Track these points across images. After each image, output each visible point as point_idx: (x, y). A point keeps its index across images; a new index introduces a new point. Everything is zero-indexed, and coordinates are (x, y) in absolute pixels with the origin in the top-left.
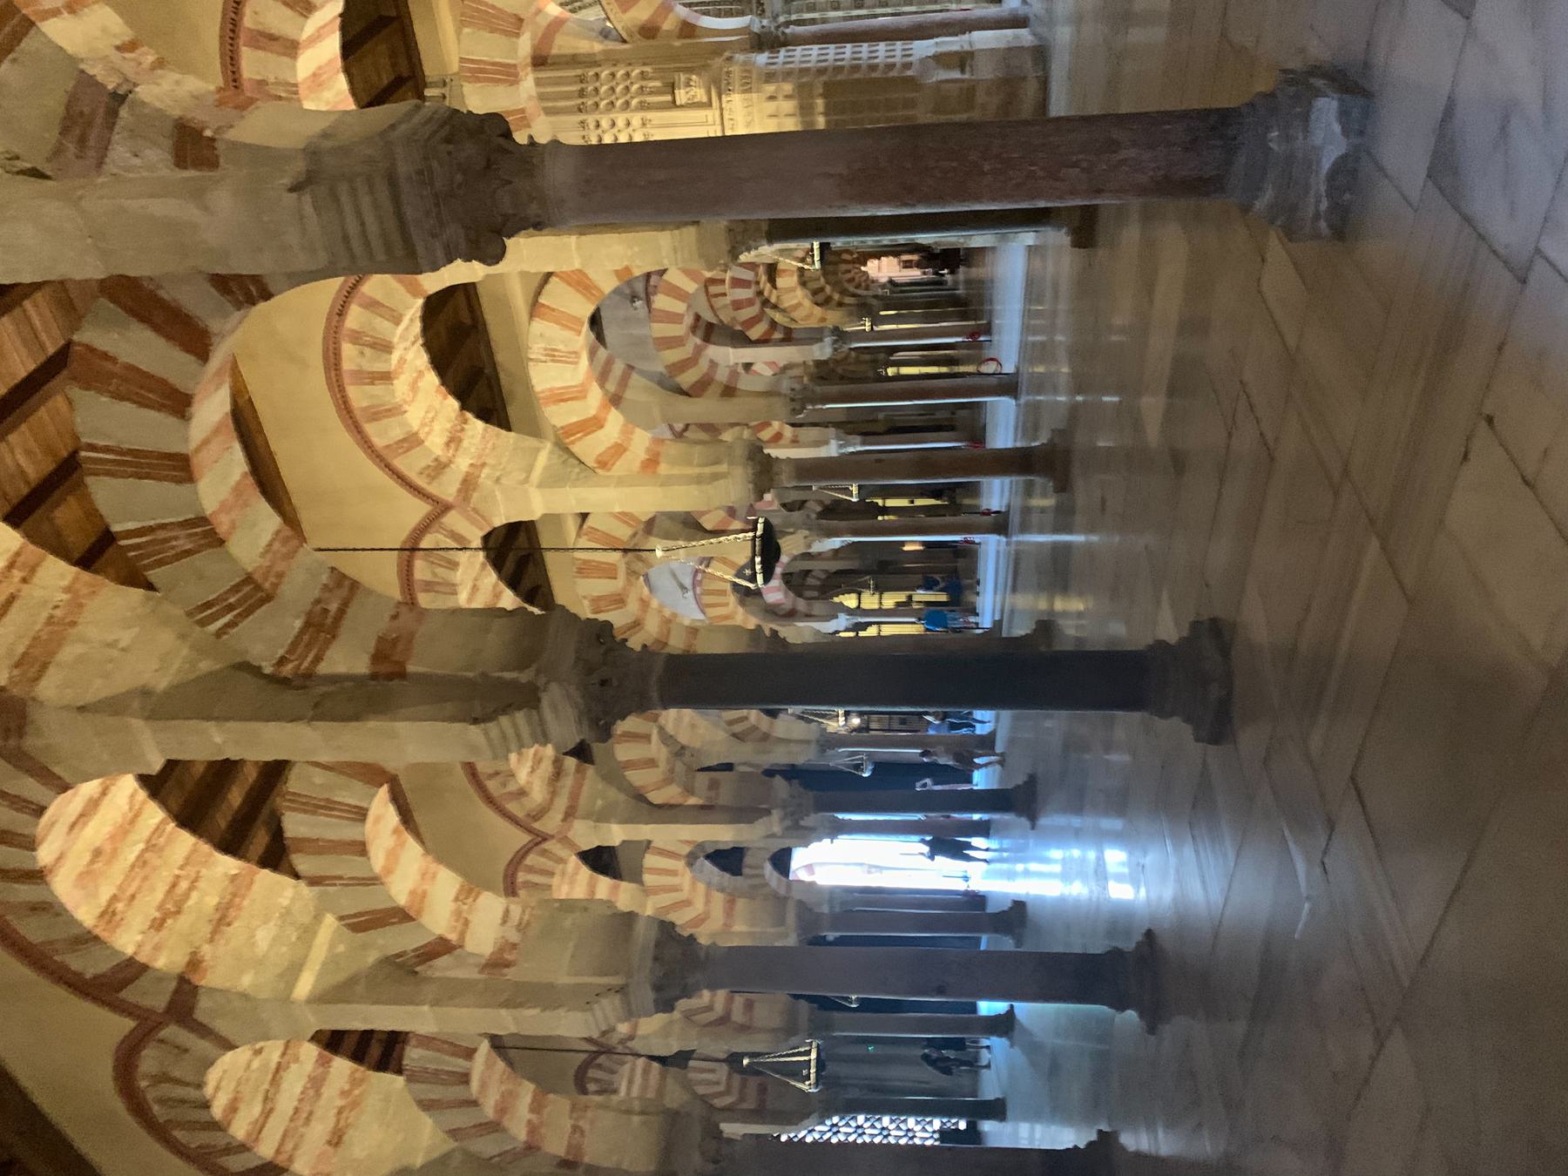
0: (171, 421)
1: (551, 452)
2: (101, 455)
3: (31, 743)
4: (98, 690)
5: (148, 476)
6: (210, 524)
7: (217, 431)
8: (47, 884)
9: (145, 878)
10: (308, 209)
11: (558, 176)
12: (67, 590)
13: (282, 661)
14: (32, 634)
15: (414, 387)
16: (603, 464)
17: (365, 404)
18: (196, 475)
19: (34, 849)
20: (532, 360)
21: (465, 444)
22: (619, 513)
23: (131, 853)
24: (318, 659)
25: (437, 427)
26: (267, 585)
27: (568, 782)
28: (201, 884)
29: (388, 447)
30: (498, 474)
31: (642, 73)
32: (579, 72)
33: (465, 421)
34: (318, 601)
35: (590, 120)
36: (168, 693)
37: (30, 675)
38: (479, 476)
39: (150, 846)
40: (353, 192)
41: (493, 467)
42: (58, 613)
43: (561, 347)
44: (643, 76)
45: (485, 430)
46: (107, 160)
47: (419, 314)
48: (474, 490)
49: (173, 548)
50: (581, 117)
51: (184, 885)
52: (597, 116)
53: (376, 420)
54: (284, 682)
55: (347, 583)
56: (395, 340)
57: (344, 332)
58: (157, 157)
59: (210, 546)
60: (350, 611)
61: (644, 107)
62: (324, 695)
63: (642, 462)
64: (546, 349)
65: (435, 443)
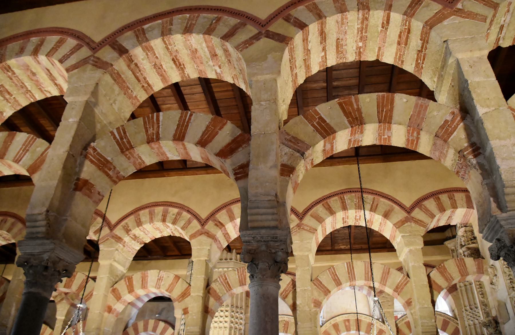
0: (197, 139)
1: (122, 272)
2: (188, 117)
3: (90, 67)
4: (102, 91)
5: (178, 128)
6: (156, 141)
7: (187, 153)
8: (30, 55)
9: (16, 85)
10: (270, 198)
11: (271, 288)
12: (136, 97)
13: (95, 149)
14: (126, 81)
15: (157, 229)
16: (114, 291)
17: (156, 211)
18: (176, 142)
19: (46, 56)
20: (160, 272)
21: (133, 242)
22: (92, 294)
23: (29, 85)
24: (92, 162)
25: (142, 233)
26: (127, 153)
28: (5, 102)
29: (139, 215)
30: (120, 251)
31: (241, 329)
32: (244, 307)
33: (141, 244)
34: (115, 168)
35: (228, 309)
36: (93, 111)
37: (114, 75)
38: (120, 243)
39: (28, 91)
40: (273, 214)
41: (122, 249)
42: (130, 91)
43: (163, 283)
44: (240, 329)
45: (136, 250)
46: (284, 146)
47: (182, 236)
48: (116, 241)
49: (150, 128)
50: (230, 305)
51: (8, 96)
52: (229, 311)
53: (150, 213)
54: (85, 148)
55: (117, 180)
56: (176, 226)
57: (182, 211)
58: (285, 160)
59: (148, 139)
60: (106, 178)
61: (231, 328)
62: (76, 161)
63: (111, 307)
64: (163, 277)
65: (137, 231)
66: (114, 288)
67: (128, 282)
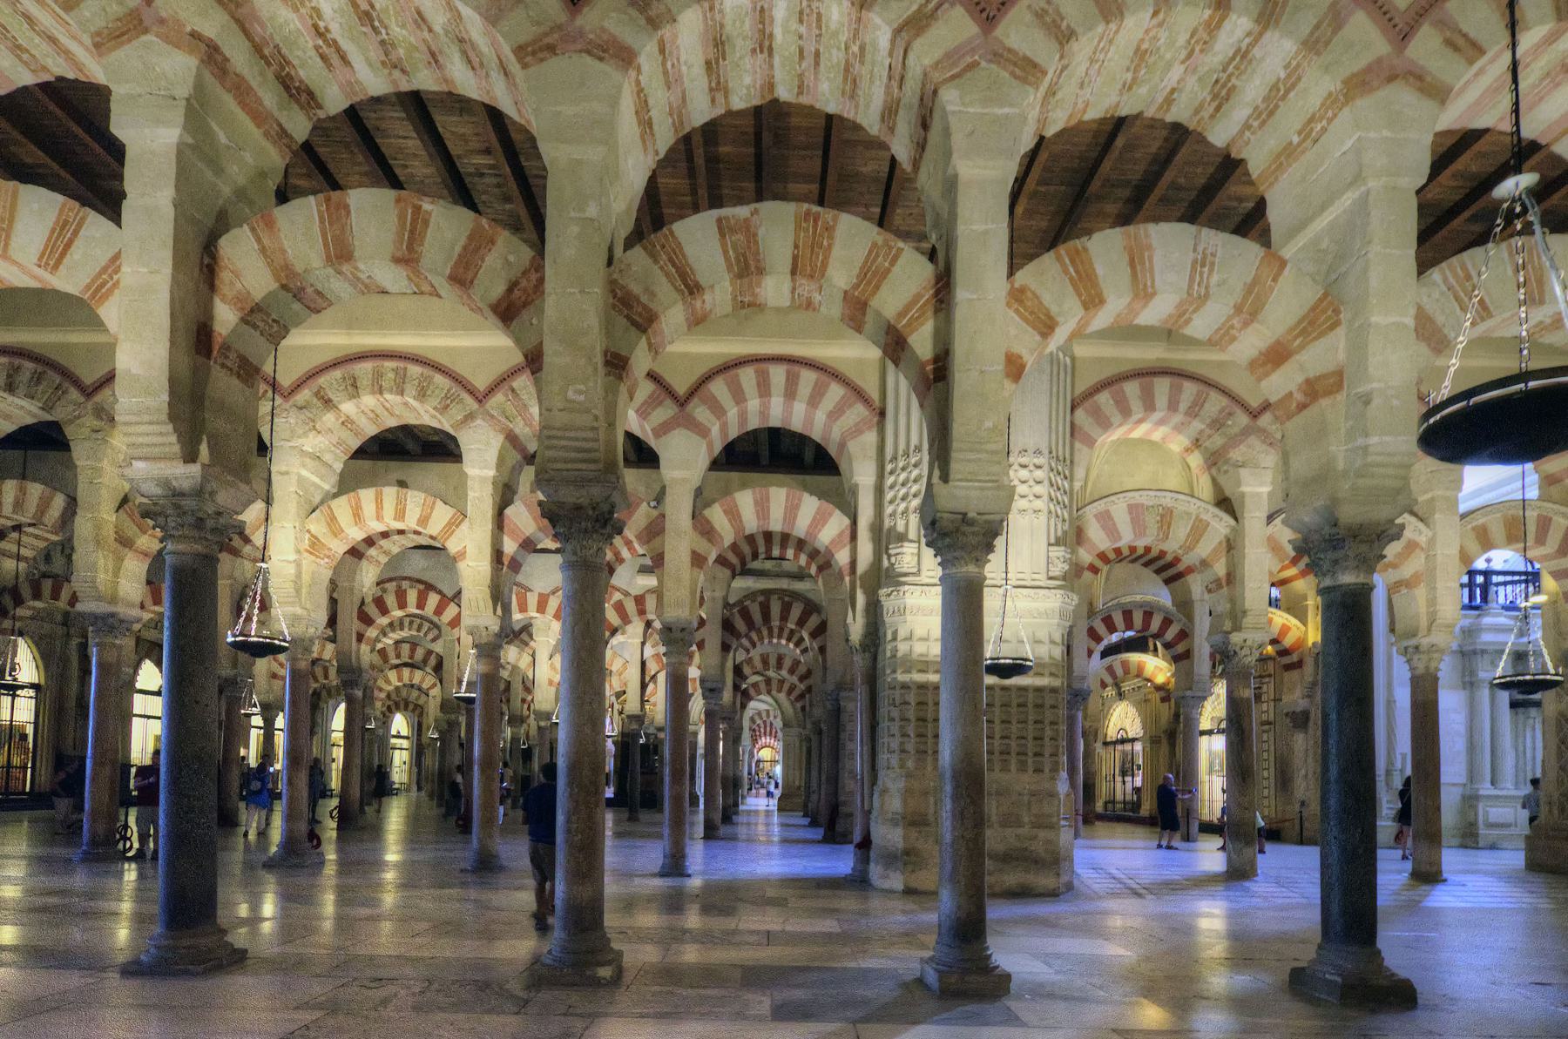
27: (269, 97)
43: (1215, 278)
48: (1013, 74)
66: (1017, 285)
67: (1073, 262)
